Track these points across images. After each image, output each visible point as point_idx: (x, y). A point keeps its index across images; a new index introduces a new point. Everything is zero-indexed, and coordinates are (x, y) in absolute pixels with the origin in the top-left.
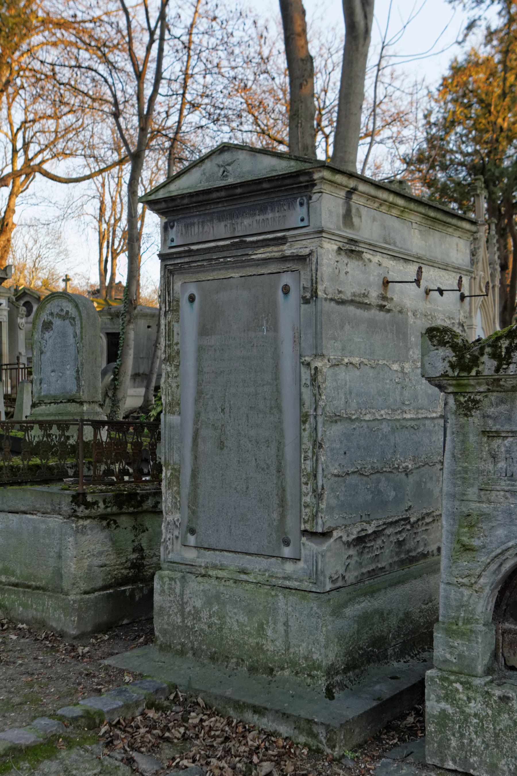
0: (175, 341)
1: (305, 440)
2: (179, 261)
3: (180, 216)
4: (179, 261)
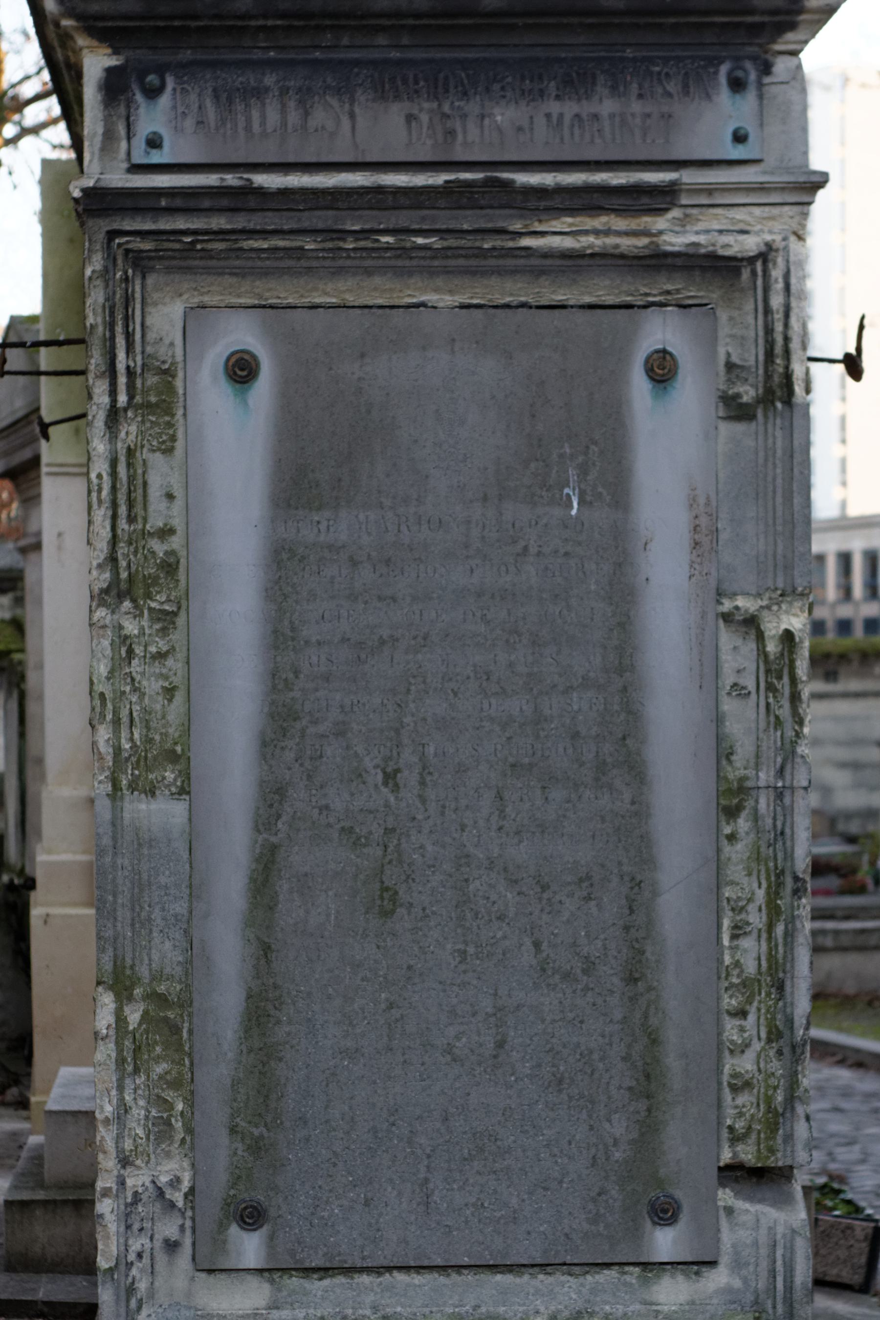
0: (156, 522)
1: (736, 872)
2: (181, 223)
3: (187, 55)
4: (181, 223)
